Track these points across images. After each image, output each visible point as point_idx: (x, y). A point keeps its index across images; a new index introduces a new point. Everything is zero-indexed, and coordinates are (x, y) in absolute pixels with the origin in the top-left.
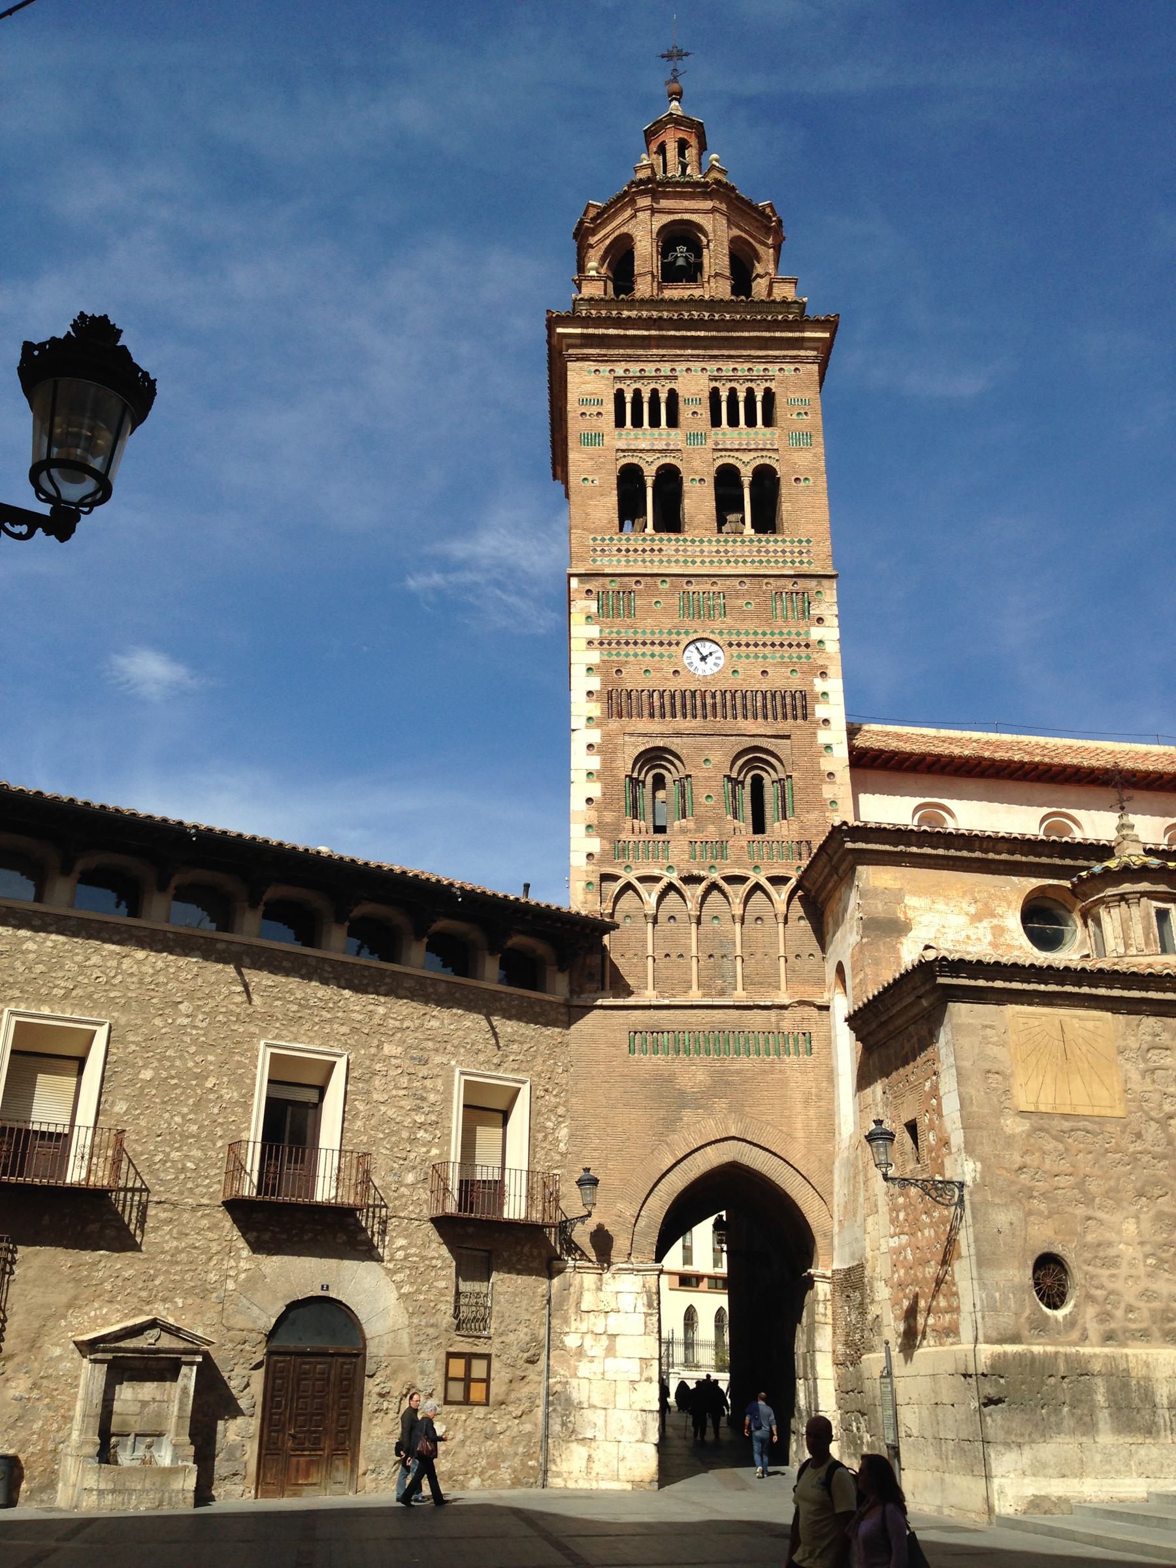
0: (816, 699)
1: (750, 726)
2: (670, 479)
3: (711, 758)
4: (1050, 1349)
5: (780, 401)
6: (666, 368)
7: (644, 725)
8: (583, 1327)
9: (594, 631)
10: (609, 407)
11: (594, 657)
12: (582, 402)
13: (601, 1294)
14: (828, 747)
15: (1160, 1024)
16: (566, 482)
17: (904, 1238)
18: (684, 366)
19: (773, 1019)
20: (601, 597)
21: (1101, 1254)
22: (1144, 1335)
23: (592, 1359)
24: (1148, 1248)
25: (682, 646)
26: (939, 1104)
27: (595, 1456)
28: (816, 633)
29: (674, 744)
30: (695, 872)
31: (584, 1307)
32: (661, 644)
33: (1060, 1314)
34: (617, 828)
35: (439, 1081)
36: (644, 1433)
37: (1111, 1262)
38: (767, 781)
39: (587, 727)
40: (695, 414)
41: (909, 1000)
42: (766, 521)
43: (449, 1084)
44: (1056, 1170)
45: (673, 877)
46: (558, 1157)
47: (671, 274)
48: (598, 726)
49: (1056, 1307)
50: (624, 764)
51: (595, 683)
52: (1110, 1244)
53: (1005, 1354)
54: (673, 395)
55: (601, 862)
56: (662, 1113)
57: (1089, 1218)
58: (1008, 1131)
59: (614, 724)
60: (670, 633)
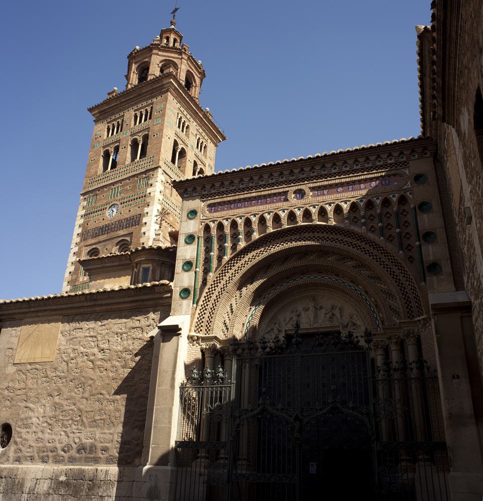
0: (144, 216)
1: (121, 232)
3: (107, 248)
5: (154, 109)
6: (122, 114)
11: (82, 221)
15: (82, 318)
21: (25, 423)
22: (32, 459)
24: (45, 419)
25: (107, 209)
39: (75, 247)
44: (20, 387)
48: (78, 245)
52: (31, 418)
57: (26, 407)
58: (7, 372)
59: (82, 244)
60: (104, 205)
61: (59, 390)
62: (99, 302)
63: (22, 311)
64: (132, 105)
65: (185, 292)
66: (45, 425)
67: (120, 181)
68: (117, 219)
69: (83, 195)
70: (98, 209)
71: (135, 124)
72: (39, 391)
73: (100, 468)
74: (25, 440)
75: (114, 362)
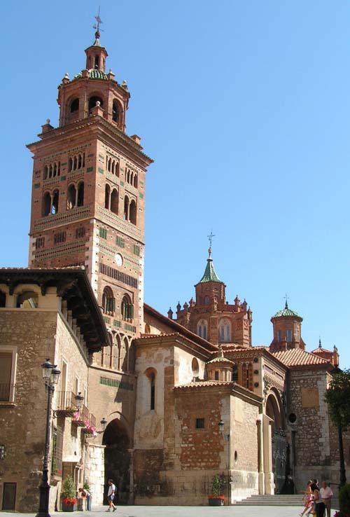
12: (100, 155)
18: (121, 156)
20: (101, 229)
28: (141, 262)
29: (112, 286)
54: (118, 165)
59: (101, 275)
69: (98, 220)
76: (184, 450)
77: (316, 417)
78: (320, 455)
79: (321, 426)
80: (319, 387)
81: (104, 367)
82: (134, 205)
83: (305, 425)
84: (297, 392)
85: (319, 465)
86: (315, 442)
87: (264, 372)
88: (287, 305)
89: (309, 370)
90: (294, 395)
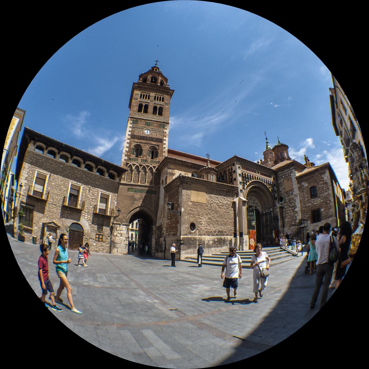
0: (164, 140)
2: (147, 107)
4: (191, 236)
5: (165, 99)
7: (136, 140)
8: (117, 232)
9: (131, 126)
10: (139, 96)
11: (130, 129)
13: (120, 228)
14: (165, 148)
16: (130, 109)
17: (169, 221)
19: (151, 188)
22: (205, 234)
23: (118, 237)
24: (206, 222)
26: (178, 200)
27: (118, 250)
28: (165, 131)
30: (141, 164)
31: (117, 229)
32: (141, 129)
33: (193, 231)
34: (130, 156)
35: (97, 192)
36: (126, 247)
37: (201, 224)
38: (154, 152)
40: (152, 98)
41: (176, 183)
42: (160, 114)
43: (98, 193)
44: (195, 210)
45: (138, 164)
46: (115, 207)
47: (152, 81)
48: (129, 140)
49: (192, 230)
50: (133, 146)
51: (130, 133)
52: (201, 222)
53: (184, 237)
54: (149, 96)
55: (127, 161)
56: (132, 201)
59: (132, 140)
61: (209, 213)
62: (220, 187)
63: (193, 182)
64: (156, 92)
65: (241, 190)
66: (207, 224)
67: (151, 121)
68: (150, 136)
69: (131, 118)
70: (139, 127)
71: (155, 99)
72: (203, 213)
73: (225, 237)
74: (201, 228)
75: (224, 207)
76: (168, 224)
77: (293, 196)
78: (296, 219)
79: (296, 201)
80: (292, 177)
81: (132, 183)
82: (161, 109)
83: (287, 202)
84: (282, 183)
85: (296, 225)
86: (293, 212)
87: (239, 171)
88: (279, 142)
89: (286, 169)
90: (281, 186)
